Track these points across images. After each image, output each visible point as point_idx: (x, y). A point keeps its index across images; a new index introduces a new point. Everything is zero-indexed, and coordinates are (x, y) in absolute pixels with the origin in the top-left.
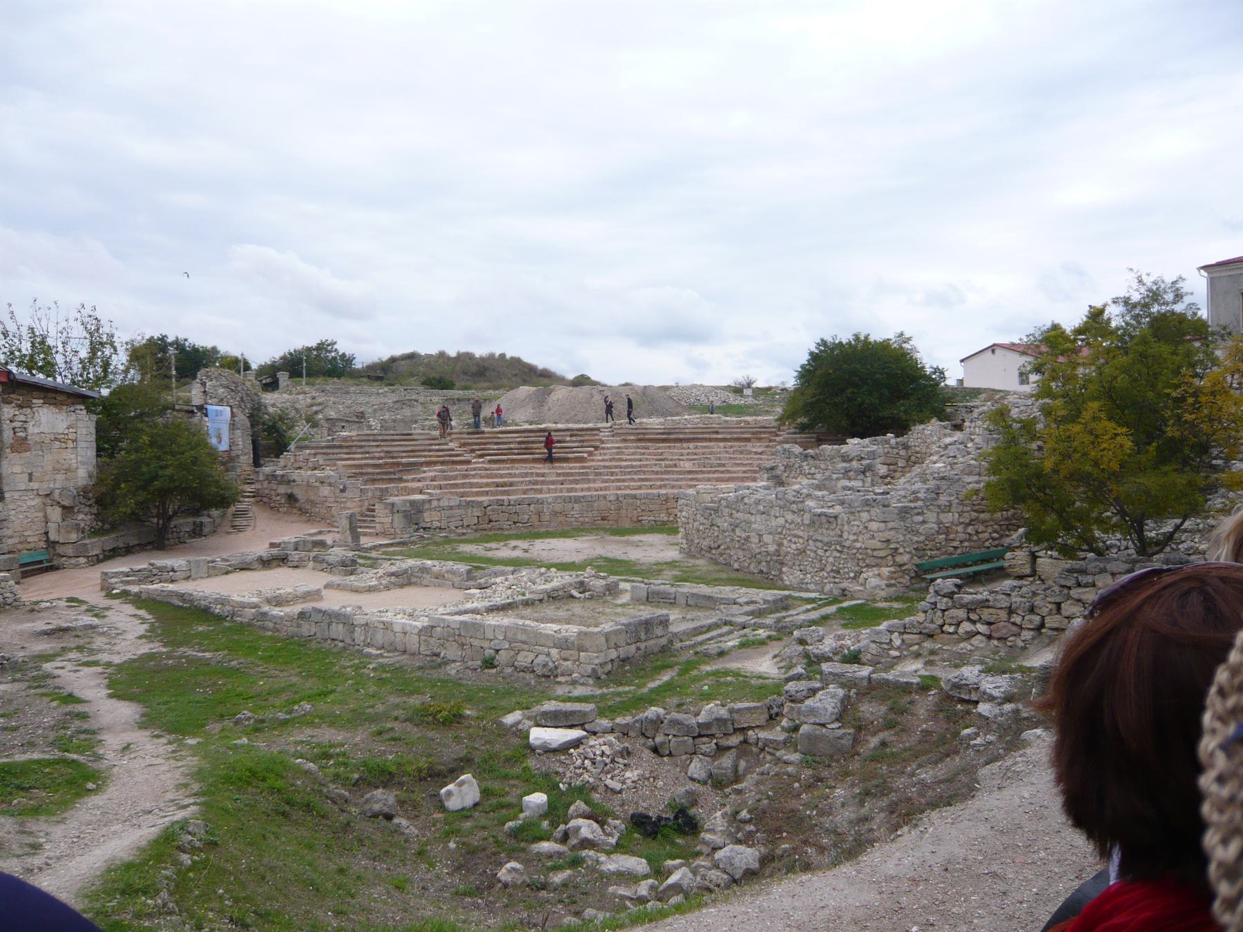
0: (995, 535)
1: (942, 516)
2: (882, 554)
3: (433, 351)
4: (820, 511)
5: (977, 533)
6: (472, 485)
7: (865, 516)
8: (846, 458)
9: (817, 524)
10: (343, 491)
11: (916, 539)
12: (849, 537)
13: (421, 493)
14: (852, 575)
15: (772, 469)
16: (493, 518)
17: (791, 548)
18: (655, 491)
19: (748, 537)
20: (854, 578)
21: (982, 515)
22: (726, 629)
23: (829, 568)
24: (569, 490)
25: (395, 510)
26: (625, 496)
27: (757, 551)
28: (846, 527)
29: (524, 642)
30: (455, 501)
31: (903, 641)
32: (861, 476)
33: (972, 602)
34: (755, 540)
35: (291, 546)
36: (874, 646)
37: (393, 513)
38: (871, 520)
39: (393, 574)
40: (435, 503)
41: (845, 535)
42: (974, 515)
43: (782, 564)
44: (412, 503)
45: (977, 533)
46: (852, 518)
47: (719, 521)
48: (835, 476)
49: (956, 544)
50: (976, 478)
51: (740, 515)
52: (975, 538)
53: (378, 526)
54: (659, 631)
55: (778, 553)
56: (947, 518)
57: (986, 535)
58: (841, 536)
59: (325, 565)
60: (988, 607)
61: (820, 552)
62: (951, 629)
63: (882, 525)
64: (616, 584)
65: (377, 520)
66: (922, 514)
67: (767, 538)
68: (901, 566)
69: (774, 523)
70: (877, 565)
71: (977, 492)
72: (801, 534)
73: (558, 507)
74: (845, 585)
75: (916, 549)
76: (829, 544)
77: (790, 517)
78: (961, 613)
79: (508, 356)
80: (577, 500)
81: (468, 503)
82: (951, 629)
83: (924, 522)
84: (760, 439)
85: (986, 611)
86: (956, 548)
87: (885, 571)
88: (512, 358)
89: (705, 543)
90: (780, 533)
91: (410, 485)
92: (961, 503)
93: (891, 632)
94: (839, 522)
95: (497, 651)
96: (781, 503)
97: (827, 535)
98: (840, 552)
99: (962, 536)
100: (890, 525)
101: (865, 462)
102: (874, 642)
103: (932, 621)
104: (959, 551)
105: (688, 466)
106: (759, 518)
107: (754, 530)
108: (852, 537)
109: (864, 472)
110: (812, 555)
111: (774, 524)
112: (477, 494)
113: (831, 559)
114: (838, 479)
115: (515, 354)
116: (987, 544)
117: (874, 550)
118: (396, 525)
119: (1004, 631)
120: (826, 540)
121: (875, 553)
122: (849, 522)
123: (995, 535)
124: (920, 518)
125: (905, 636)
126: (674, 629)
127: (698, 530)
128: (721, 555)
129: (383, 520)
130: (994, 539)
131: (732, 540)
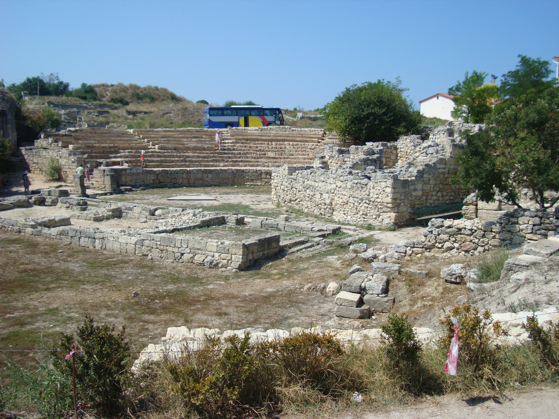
0: (451, 198)
5: (443, 196)
7: (383, 184)
12: (373, 196)
14: (374, 217)
15: (323, 157)
16: (162, 180)
17: (338, 201)
19: (314, 195)
20: (376, 219)
21: (446, 187)
23: (361, 213)
25: (106, 173)
27: (319, 202)
28: (372, 191)
29: (199, 249)
33: (452, 232)
35: (47, 193)
36: (397, 254)
37: (104, 176)
38: (386, 187)
40: (128, 171)
41: (371, 195)
43: (333, 210)
46: (376, 185)
47: (296, 185)
49: (431, 201)
50: (443, 166)
51: (309, 182)
52: (441, 199)
54: (274, 245)
55: (331, 204)
56: (427, 187)
57: (447, 198)
58: (369, 195)
60: (461, 234)
61: (356, 204)
62: (440, 246)
64: (243, 218)
66: (414, 184)
67: (325, 196)
69: (329, 187)
71: (443, 173)
72: (346, 193)
74: (371, 221)
76: (362, 200)
77: (339, 184)
78: (445, 237)
82: (440, 246)
84: (313, 142)
85: (459, 236)
89: (288, 198)
90: (333, 193)
91: (113, 160)
93: (407, 247)
94: (368, 187)
95: (182, 254)
96: (334, 176)
98: (369, 204)
99: (435, 198)
102: (397, 252)
103: (429, 241)
105: (271, 154)
106: (320, 184)
108: (375, 196)
110: (352, 205)
113: (363, 208)
115: (164, 86)
116: (448, 202)
117: (388, 203)
119: (469, 247)
120: (360, 197)
121: (389, 205)
122: (373, 188)
125: (414, 249)
126: (282, 243)
127: (284, 190)
128: (297, 204)
130: (451, 200)
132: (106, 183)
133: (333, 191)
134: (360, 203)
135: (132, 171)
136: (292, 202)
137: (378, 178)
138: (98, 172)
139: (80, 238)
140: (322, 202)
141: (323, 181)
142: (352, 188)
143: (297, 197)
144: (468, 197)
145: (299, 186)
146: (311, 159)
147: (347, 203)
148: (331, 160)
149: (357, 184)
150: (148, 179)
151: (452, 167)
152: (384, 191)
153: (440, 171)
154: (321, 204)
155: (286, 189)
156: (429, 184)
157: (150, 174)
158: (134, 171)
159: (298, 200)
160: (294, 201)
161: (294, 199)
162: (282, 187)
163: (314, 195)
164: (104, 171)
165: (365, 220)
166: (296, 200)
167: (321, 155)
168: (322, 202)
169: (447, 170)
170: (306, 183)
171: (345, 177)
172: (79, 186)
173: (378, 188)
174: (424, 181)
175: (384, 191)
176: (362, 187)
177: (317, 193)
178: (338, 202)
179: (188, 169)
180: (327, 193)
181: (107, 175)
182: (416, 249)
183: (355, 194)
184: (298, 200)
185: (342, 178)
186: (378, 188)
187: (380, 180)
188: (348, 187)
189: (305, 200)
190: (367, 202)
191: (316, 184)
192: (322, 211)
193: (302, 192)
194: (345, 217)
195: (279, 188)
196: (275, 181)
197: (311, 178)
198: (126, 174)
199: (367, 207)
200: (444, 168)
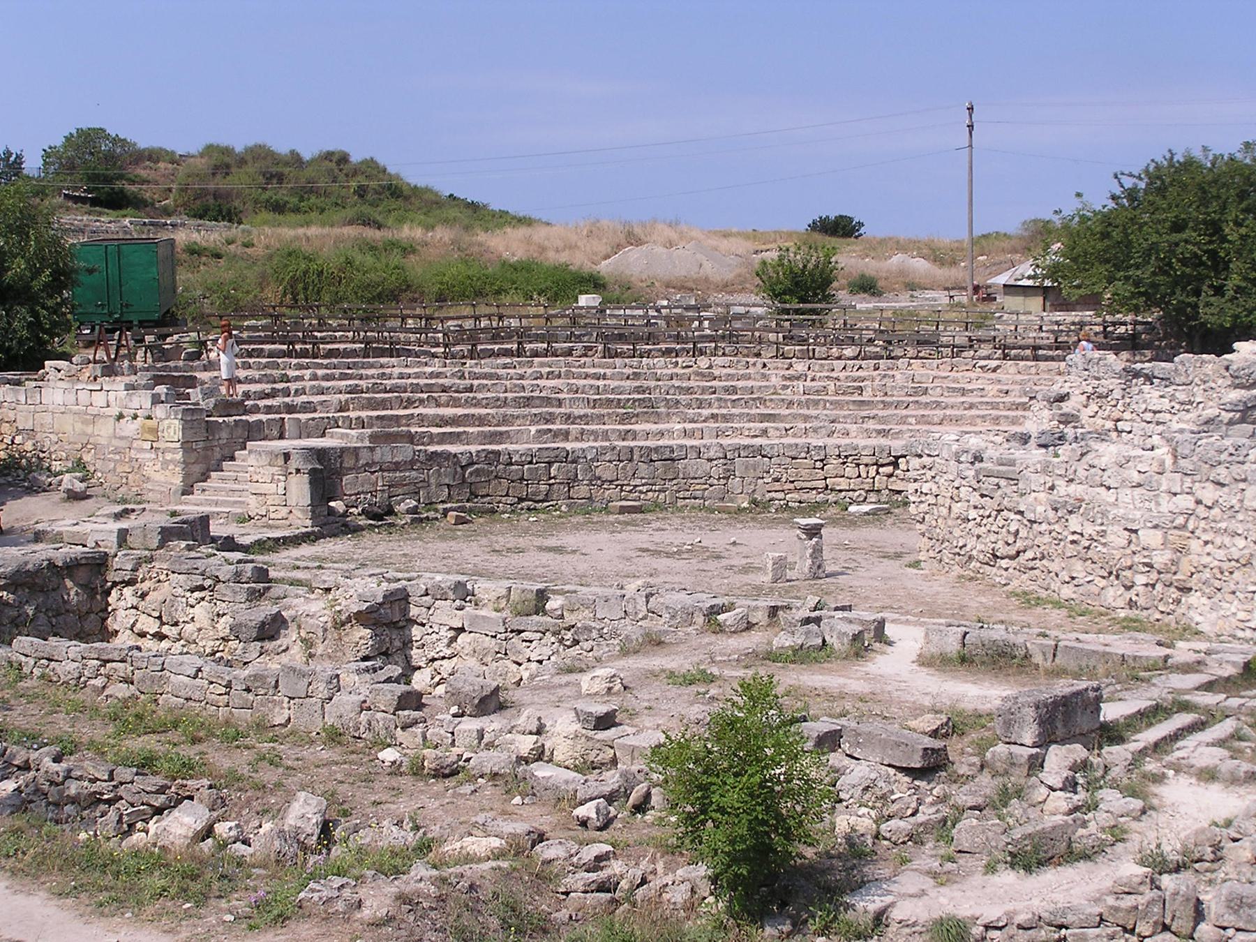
6: (422, 420)
15: (1062, 398)
22: (1182, 719)
24: (624, 435)
25: (294, 464)
26: (737, 449)
35: (114, 538)
37: (287, 475)
44: (320, 454)
51: (1075, 489)
67: (1149, 537)
69: (1166, 505)
77: (1208, 494)
80: (649, 456)
90: (1183, 527)
106: (1126, 495)
112: (443, 438)
132: (292, 501)
133: (1180, 520)
135: (377, 456)
136: (1004, 563)
138: (265, 460)
140: (1137, 559)
141: (1139, 485)
143: (1020, 544)
145: (1037, 504)
146: (1017, 406)
148: (1093, 407)
155: (973, 514)
158: (384, 454)
159: (1029, 554)
160: (1012, 558)
162: (957, 508)
163: (1103, 534)
164: (287, 456)
166: (1018, 553)
167: (1058, 388)
168: (1137, 559)
170: (1062, 488)
177: (1117, 528)
179: (569, 446)
180: (1156, 527)
181: (298, 471)
184: (1029, 554)
185: (1221, 470)
189: (1063, 556)
191: (1109, 496)
193: (1044, 527)
194: (1242, 615)
195: (944, 511)
197: (1081, 473)
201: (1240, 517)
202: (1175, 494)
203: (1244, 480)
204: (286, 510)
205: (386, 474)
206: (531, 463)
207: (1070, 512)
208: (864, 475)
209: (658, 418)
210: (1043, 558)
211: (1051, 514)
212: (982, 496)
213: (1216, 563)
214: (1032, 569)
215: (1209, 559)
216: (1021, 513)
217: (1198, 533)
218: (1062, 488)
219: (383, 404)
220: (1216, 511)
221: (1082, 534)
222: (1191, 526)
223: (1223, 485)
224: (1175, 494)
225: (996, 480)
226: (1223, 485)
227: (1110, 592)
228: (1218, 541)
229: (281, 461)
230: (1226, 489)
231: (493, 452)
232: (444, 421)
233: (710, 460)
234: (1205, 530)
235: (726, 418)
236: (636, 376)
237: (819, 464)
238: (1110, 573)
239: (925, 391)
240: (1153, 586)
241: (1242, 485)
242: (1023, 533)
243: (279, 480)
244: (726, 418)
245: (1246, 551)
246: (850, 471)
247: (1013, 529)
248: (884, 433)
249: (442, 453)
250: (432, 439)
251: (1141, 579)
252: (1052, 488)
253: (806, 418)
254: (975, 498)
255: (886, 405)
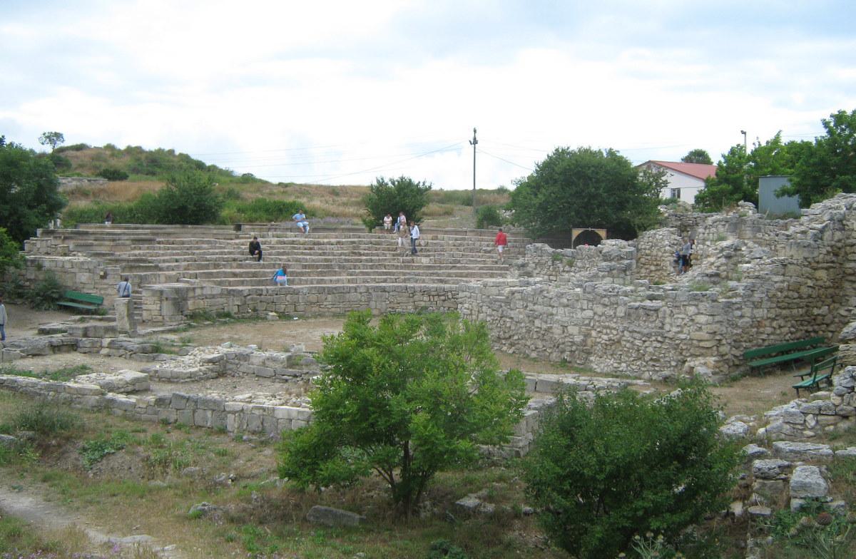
0: (792, 329)
1: (755, 311)
2: (708, 344)
3: (101, 144)
4: (637, 304)
7: (692, 310)
8: (607, 258)
9: (634, 316)
10: (104, 277)
11: (735, 331)
13: (178, 281)
14: (673, 363)
15: (523, 266)
18: (403, 285)
23: (647, 358)
24: (319, 282)
25: (164, 296)
26: (375, 289)
28: (668, 320)
30: (217, 290)
31: (817, 422)
32: (622, 275)
34: (557, 330)
35: (80, 332)
36: (788, 426)
37: (161, 301)
38: (699, 313)
39: (210, 361)
40: (198, 292)
41: (667, 327)
42: (779, 311)
43: (589, 353)
44: (177, 291)
45: (780, 327)
46: (676, 311)
47: (512, 313)
48: (601, 274)
49: (764, 336)
50: (781, 278)
53: (145, 314)
55: (584, 343)
56: (760, 313)
58: (661, 328)
59: (122, 351)
63: (711, 318)
65: (144, 307)
68: (722, 356)
70: (701, 355)
73: (313, 298)
75: (735, 341)
76: (649, 335)
77: (600, 309)
79: (177, 153)
80: (331, 291)
81: (229, 292)
83: (742, 316)
86: (764, 340)
87: (711, 360)
88: (181, 154)
90: (589, 325)
92: (770, 299)
93: (805, 414)
96: (591, 297)
97: (645, 327)
99: (769, 330)
100: (717, 318)
101: (626, 262)
103: (849, 404)
104: (766, 343)
106: (561, 310)
107: (557, 321)
108: (675, 329)
109: (625, 271)
111: (579, 316)
114: (604, 277)
116: (787, 337)
118: (165, 312)
120: (646, 331)
122: (672, 315)
123: (792, 329)
124: (738, 313)
125: (820, 418)
129: (150, 307)
130: (792, 333)
131: (529, 331)
133: (587, 322)
134: (644, 341)
137: (681, 299)
139: (194, 412)
141: (568, 306)
142: (628, 315)
143: (511, 333)
144: (845, 330)
147: (619, 342)
149: (637, 309)
150: (231, 304)
151: (793, 280)
152: (692, 320)
153: (777, 285)
154: (563, 343)
156: (761, 308)
157: (234, 296)
159: (516, 337)
161: (507, 335)
165: (656, 368)
166: (510, 337)
167: (520, 261)
169: (786, 284)
170: (531, 306)
171: (613, 299)
172: (126, 319)
173: (680, 316)
174: (753, 303)
175: (692, 320)
176: (648, 315)
178: (598, 340)
179: (294, 287)
180: (575, 325)
182: (823, 417)
183: (632, 328)
184: (516, 337)
185: (606, 299)
186: (680, 316)
187: (685, 303)
188: (618, 314)
189: (532, 338)
190: (659, 338)
192: (566, 355)
193: (523, 325)
194: (615, 365)
196: (466, 305)
197: (540, 300)
198: (194, 297)
199: (660, 347)
200: (783, 282)
201: (615, 320)
202: (585, 310)
203: (617, 304)
204: (161, 317)
205: (208, 300)
206: (277, 294)
207: (536, 318)
208: (432, 300)
209: (335, 273)
210: (522, 339)
211: (526, 319)
212: (494, 310)
213: (604, 341)
214: (518, 344)
215: (600, 340)
216: (512, 318)
217: (595, 327)
218: (531, 306)
219: (207, 267)
220: (603, 318)
221: (541, 328)
222: (592, 324)
223: (607, 306)
224: (585, 310)
225: (499, 303)
226: (607, 306)
227: (554, 355)
228: (605, 331)
229: (158, 294)
230: (608, 308)
231: (259, 290)
232: (235, 275)
233: (361, 293)
234: (598, 327)
235: (368, 274)
236: (324, 254)
237: (411, 295)
238: (554, 346)
239: (459, 262)
240: (574, 351)
241: (615, 306)
242: (513, 328)
243: (157, 304)
244: (368, 274)
245: (618, 336)
246: (426, 298)
247: (508, 325)
248: (441, 281)
249: (234, 290)
250: (230, 284)
251: (569, 348)
252: (527, 307)
253: (404, 274)
254: (489, 311)
255: (441, 268)
